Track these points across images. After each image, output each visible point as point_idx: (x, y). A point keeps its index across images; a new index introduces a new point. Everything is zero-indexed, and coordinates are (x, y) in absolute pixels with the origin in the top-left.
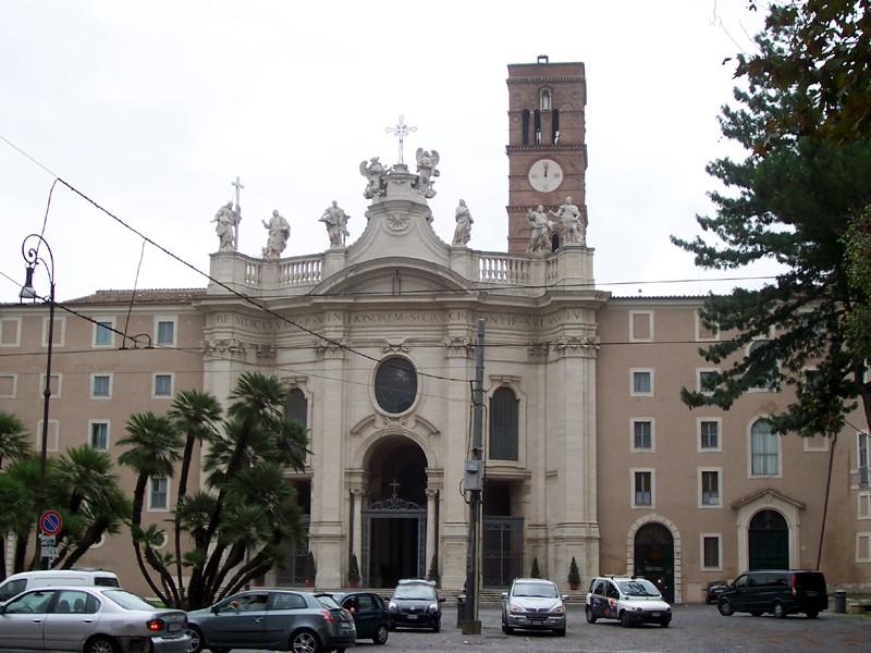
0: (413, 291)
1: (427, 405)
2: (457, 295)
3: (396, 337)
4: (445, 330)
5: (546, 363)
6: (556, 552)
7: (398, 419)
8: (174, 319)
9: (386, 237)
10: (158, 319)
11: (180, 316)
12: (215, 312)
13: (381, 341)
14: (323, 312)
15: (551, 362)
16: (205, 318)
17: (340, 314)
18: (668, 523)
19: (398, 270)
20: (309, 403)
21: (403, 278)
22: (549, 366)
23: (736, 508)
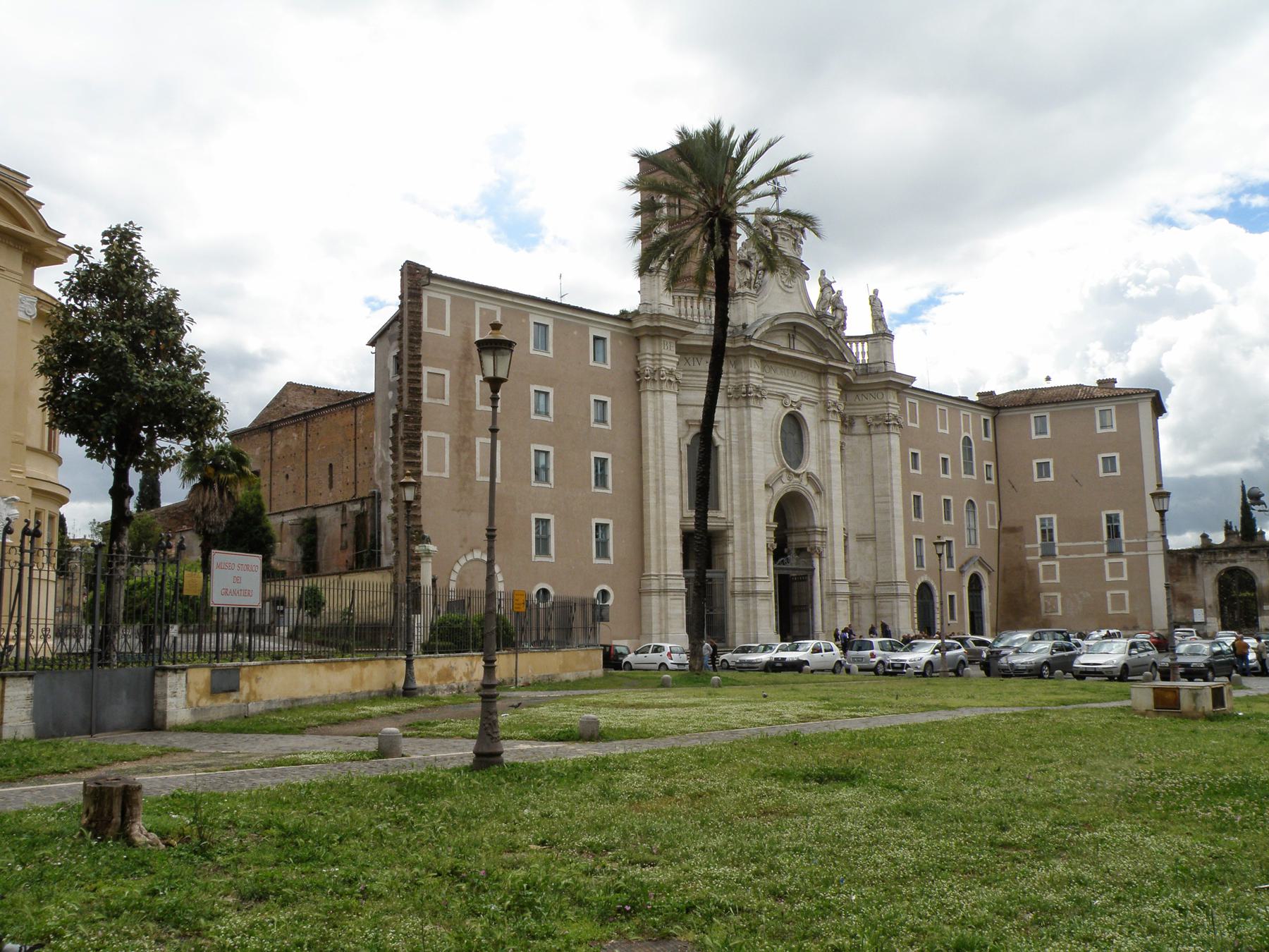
0: (801, 349)
1: (811, 465)
2: (838, 361)
3: (796, 395)
4: (823, 391)
5: (852, 435)
6: (876, 608)
7: (798, 475)
8: (606, 334)
9: (780, 291)
10: (594, 331)
11: (612, 333)
12: (660, 336)
13: (784, 396)
14: (749, 355)
15: (855, 435)
16: (638, 339)
17: (758, 360)
18: (932, 583)
19: (795, 325)
20: (721, 450)
21: (798, 337)
22: (855, 438)
23: (961, 572)
